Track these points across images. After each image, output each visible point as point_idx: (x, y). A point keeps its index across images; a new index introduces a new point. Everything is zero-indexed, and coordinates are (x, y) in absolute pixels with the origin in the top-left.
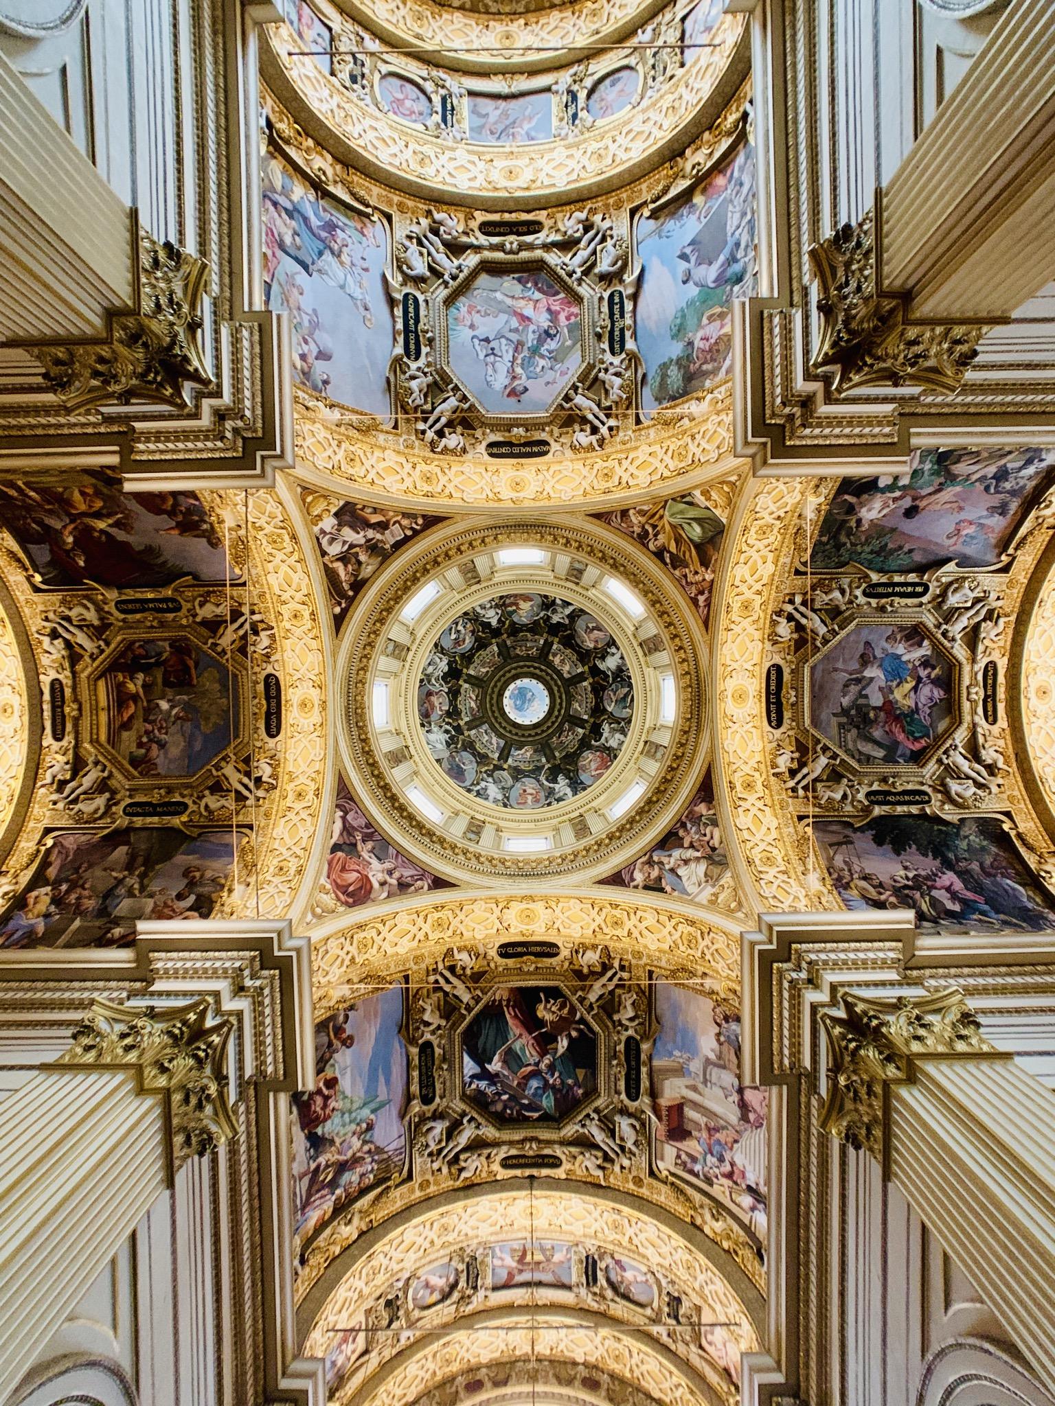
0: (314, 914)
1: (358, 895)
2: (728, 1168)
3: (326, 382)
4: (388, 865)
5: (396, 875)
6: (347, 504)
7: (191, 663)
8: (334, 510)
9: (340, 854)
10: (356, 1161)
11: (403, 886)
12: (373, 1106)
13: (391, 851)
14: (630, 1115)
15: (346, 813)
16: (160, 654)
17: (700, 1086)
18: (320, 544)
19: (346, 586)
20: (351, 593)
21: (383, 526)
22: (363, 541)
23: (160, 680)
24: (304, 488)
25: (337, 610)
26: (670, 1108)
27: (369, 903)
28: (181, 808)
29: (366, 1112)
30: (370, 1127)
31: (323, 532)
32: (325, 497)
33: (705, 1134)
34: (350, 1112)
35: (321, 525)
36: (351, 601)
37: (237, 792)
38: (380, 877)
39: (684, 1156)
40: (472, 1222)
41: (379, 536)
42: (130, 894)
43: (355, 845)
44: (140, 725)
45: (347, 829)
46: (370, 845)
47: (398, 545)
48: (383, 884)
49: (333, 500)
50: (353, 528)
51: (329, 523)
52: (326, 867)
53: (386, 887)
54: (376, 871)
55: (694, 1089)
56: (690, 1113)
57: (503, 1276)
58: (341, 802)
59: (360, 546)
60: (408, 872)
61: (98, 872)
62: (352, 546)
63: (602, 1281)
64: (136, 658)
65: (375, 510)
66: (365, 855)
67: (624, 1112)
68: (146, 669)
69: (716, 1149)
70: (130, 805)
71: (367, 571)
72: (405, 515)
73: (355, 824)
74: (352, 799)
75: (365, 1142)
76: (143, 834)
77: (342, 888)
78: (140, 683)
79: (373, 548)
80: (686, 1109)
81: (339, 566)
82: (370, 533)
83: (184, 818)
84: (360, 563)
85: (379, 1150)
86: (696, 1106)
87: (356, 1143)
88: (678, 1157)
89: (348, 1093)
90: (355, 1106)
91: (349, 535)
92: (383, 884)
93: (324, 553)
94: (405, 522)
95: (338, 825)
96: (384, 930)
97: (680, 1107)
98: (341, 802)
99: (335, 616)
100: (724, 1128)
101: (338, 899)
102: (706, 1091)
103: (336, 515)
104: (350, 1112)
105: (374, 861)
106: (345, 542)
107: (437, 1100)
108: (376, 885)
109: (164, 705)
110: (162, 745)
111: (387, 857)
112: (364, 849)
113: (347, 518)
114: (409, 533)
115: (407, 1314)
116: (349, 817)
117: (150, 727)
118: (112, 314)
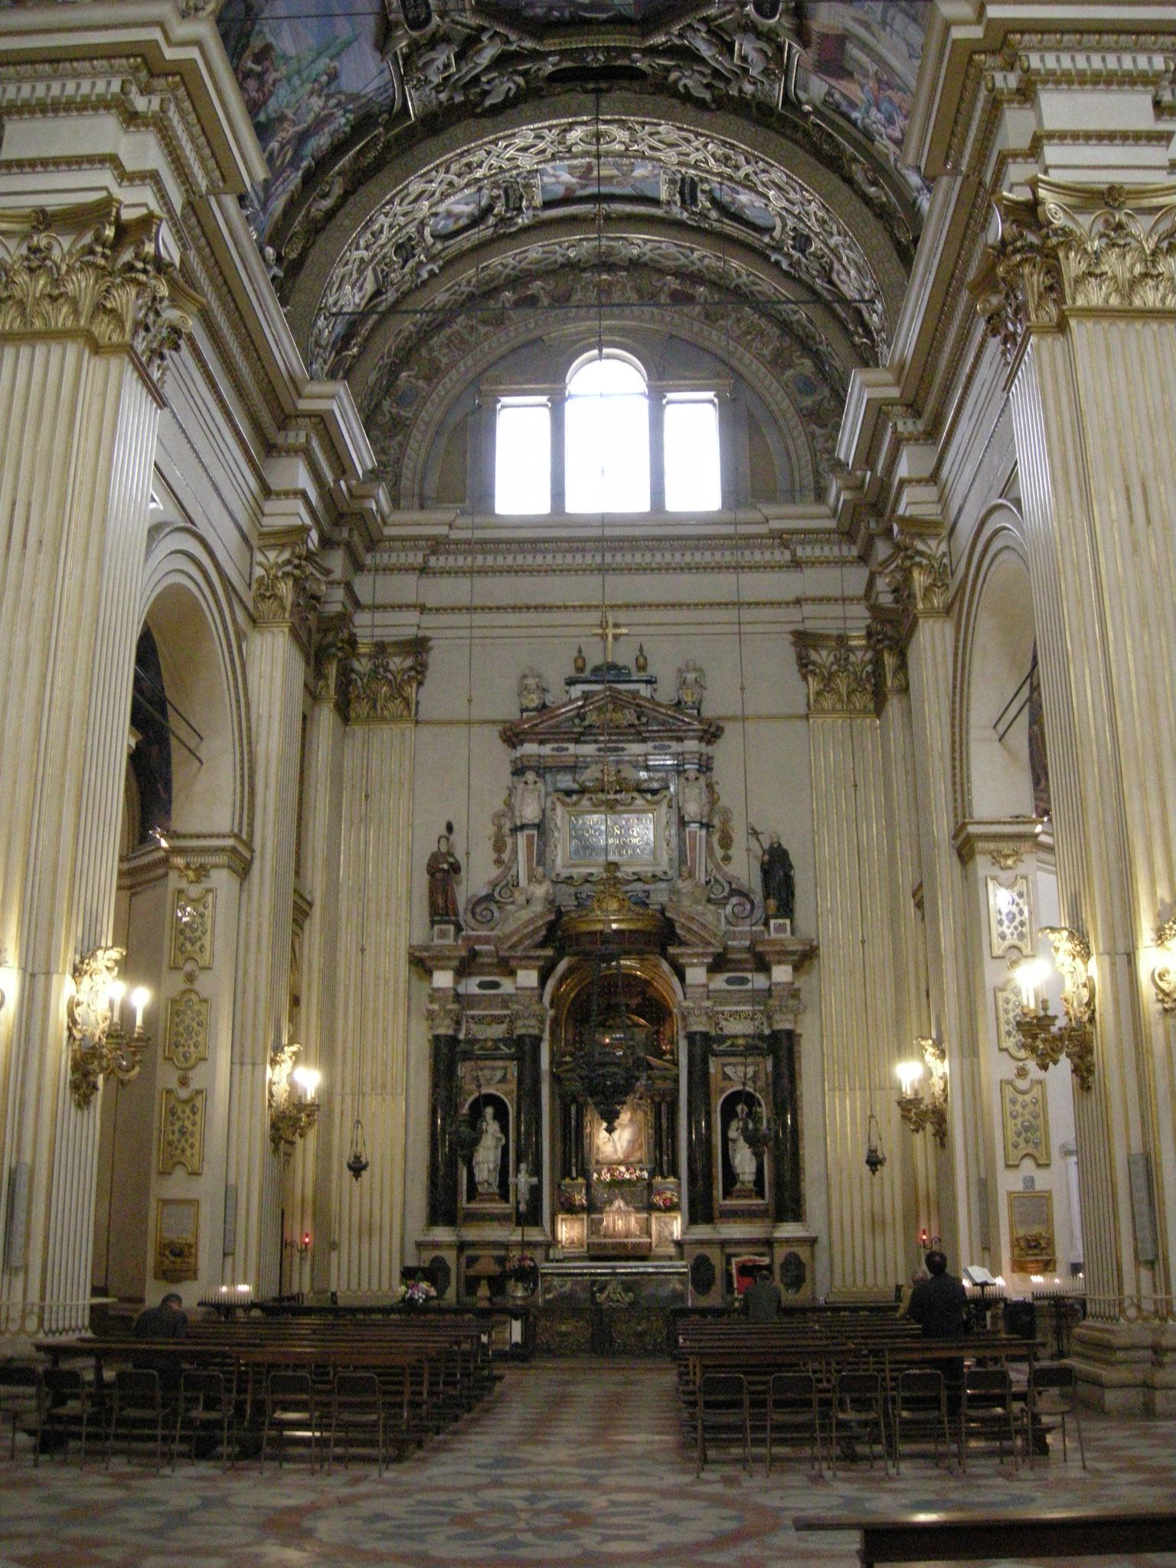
2: (897, 134)
10: (321, 122)
12: (333, 50)
14: (759, 35)
17: (876, 27)
26: (825, 37)
29: (323, 63)
30: (333, 76)
33: (871, 84)
34: (299, 73)
39: (837, 96)
40: (510, 152)
55: (867, 26)
56: (854, 51)
57: (560, 191)
63: (703, 201)
67: (748, 28)
69: (885, 106)
75: (329, 97)
80: (849, 46)
85: (353, 97)
86: (865, 47)
87: (317, 103)
88: (829, 94)
89: (291, 51)
90: (304, 63)
97: (842, 39)
100: (900, 89)
102: (884, 36)
104: (299, 73)
107: (436, 19)
115: (427, 250)
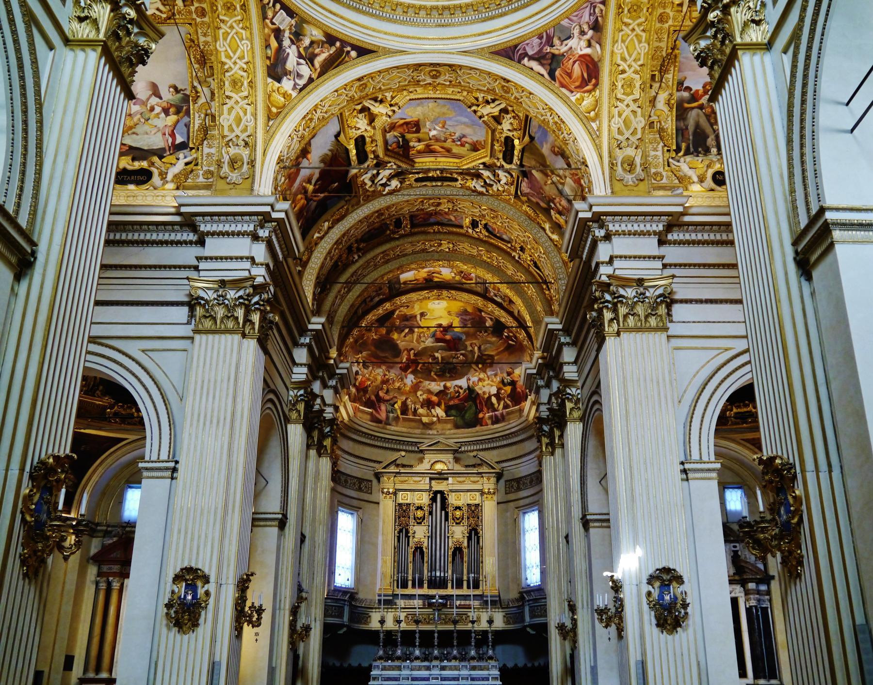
0: (594, 120)
1: (592, 69)
3: (177, 90)
4: (576, 32)
5: (585, 27)
6: (270, 75)
7: (402, 122)
8: (277, 84)
9: (557, 73)
11: (597, 27)
13: (565, 22)
15: (526, 54)
16: (395, 137)
18: (305, 86)
19: (333, 50)
20: (338, 44)
21: (278, 33)
22: (294, 47)
23: (415, 135)
24: (269, 119)
25: (353, 54)
27: (599, 64)
28: (509, 142)
31: (294, 88)
32: (270, 96)
35: (290, 92)
36: (344, 43)
37: (501, 111)
38: (583, 44)
41: (287, 34)
42: (563, 184)
43: (554, 55)
44: (448, 144)
45: (539, 58)
46: (556, 41)
47: (291, 13)
48: (589, 45)
49: (269, 89)
50: (285, 60)
51: (287, 84)
52: (564, 90)
53: (593, 43)
54: (578, 46)
58: (516, 57)
59: (298, 48)
60: (586, 17)
61: (547, 188)
62: (300, 56)
64: (399, 146)
65: (268, 46)
66: (563, 49)
68: (406, 142)
70: (505, 159)
71: (317, 34)
72: (264, 17)
73: (536, 49)
74: (516, 46)
76: (525, 159)
77: (584, 83)
78: (417, 144)
79: (297, 36)
81: (318, 61)
82: (286, 42)
83: (516, 142)
84: (312, 43)
91: (292, 62)
92: (589, 45)
93: (311, 80)
94: (270, 14)
95: (534, 65)
96: (623, 66)
98: (516, 57)
99: (359, 56)
101: (590, 91)
103: (279, 80)
105: (572, 43)
106: (298, 64)
108: (588, 51)
109: (433, 133)
110: (464, 136)
111: (569, 29)
112: (560, 48)
113: (279, 70)
114: (278, 6)
116: (530, 53)
117: (449, 140)
118: (244, 336)
